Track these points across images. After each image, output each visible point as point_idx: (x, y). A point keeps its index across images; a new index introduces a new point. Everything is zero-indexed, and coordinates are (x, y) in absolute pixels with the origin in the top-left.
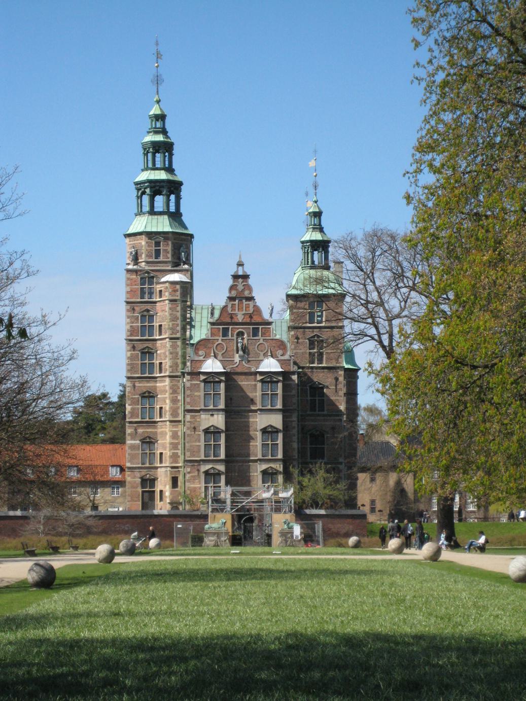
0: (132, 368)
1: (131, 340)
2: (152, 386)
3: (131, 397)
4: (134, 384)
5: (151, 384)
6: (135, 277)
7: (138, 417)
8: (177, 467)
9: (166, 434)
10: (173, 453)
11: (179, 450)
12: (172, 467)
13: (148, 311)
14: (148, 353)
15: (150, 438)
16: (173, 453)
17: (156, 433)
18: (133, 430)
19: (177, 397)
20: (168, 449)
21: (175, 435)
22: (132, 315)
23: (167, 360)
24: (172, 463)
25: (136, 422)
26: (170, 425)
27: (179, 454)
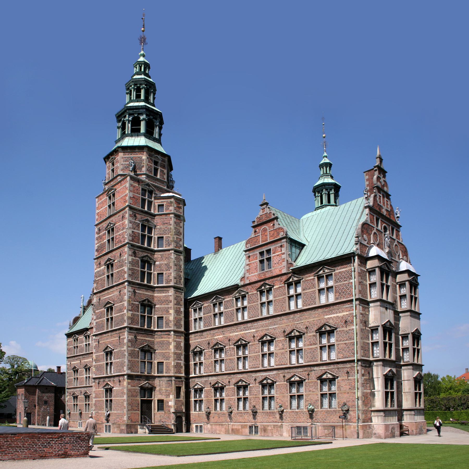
0: (133, 273)
1: (132, 245)
2: (150, 295)
3: (132, 302)
4: (134, 290)
5: (149, 293)
6: (137, 185)
7: (137, 324)
8: (180, 378)
9: (169, 343)
10: (177, 363)
11: (181, 360)
12: (177, 377)
13: (147, 220)
14: (147, 262)
15: (149, 346)
16: (177, 363)
17: (153, 342)
18: (133, 337)
19: (180, 308)
20: (172, 359)
21: (177, 347)
22: (134, 221)
23: (172, 271)
24: (176, 373)
25: (136, 329)
26: (174, 335)
27: (182, 365)
